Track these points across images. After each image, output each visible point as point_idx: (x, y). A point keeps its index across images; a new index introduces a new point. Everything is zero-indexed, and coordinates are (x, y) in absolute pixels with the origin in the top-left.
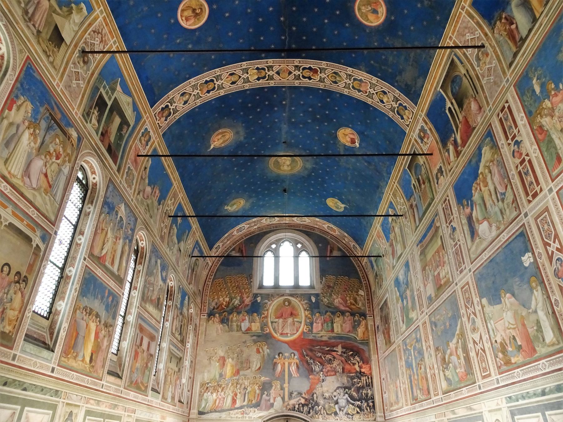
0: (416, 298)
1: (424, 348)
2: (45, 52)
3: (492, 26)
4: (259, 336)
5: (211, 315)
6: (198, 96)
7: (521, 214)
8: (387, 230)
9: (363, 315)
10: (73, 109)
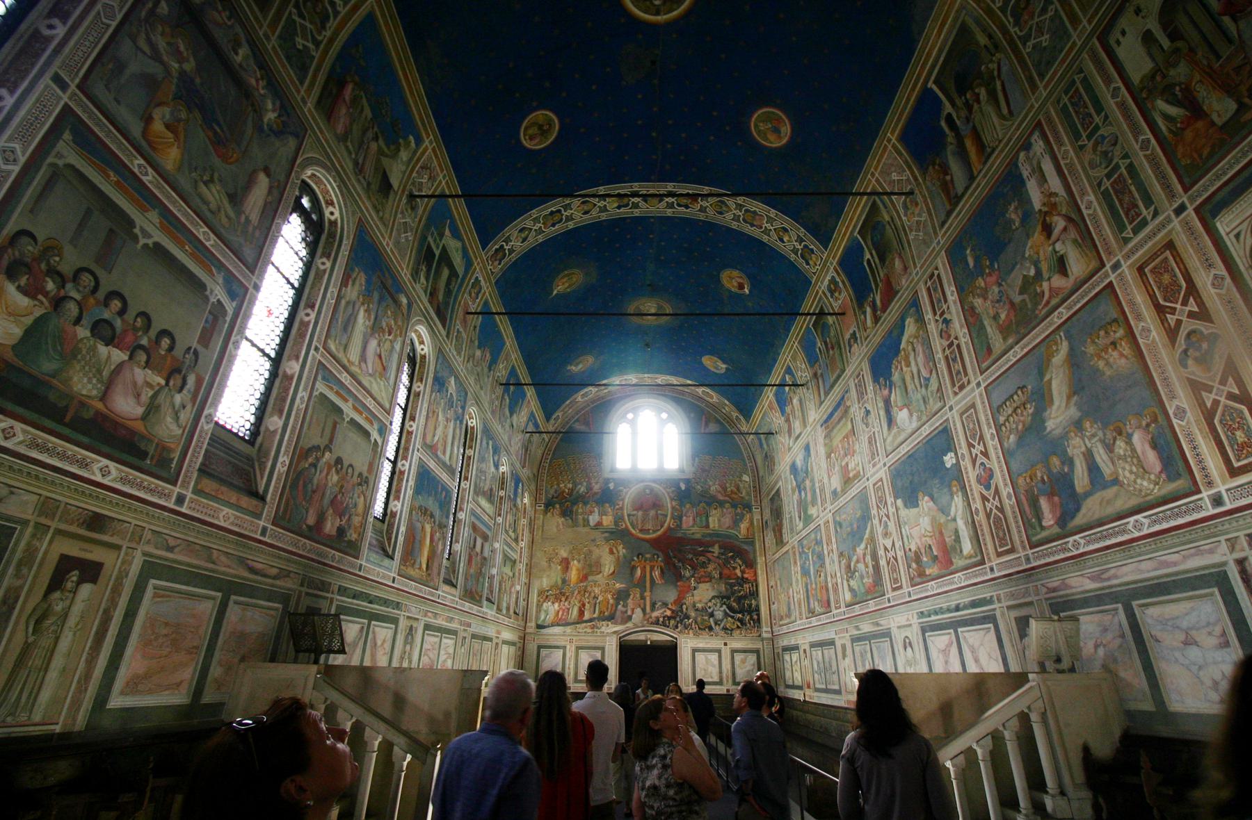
0: (818, 491)
1: (826, 552)
2: (375, 207)
3: (924, 171)
4: (612, 533)
5: (549, 505)
6: (540, 231)
7: (945, 406)
8: (782, 402)
9: (748, 507)
10: (402, 269)
